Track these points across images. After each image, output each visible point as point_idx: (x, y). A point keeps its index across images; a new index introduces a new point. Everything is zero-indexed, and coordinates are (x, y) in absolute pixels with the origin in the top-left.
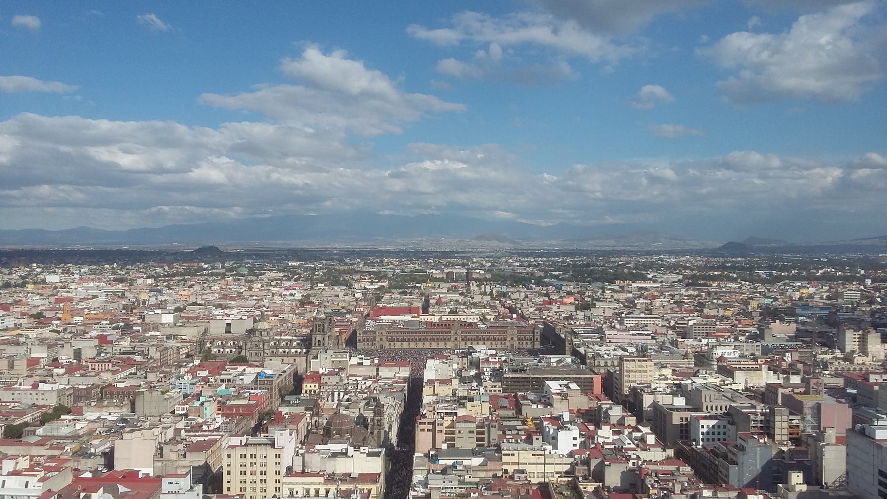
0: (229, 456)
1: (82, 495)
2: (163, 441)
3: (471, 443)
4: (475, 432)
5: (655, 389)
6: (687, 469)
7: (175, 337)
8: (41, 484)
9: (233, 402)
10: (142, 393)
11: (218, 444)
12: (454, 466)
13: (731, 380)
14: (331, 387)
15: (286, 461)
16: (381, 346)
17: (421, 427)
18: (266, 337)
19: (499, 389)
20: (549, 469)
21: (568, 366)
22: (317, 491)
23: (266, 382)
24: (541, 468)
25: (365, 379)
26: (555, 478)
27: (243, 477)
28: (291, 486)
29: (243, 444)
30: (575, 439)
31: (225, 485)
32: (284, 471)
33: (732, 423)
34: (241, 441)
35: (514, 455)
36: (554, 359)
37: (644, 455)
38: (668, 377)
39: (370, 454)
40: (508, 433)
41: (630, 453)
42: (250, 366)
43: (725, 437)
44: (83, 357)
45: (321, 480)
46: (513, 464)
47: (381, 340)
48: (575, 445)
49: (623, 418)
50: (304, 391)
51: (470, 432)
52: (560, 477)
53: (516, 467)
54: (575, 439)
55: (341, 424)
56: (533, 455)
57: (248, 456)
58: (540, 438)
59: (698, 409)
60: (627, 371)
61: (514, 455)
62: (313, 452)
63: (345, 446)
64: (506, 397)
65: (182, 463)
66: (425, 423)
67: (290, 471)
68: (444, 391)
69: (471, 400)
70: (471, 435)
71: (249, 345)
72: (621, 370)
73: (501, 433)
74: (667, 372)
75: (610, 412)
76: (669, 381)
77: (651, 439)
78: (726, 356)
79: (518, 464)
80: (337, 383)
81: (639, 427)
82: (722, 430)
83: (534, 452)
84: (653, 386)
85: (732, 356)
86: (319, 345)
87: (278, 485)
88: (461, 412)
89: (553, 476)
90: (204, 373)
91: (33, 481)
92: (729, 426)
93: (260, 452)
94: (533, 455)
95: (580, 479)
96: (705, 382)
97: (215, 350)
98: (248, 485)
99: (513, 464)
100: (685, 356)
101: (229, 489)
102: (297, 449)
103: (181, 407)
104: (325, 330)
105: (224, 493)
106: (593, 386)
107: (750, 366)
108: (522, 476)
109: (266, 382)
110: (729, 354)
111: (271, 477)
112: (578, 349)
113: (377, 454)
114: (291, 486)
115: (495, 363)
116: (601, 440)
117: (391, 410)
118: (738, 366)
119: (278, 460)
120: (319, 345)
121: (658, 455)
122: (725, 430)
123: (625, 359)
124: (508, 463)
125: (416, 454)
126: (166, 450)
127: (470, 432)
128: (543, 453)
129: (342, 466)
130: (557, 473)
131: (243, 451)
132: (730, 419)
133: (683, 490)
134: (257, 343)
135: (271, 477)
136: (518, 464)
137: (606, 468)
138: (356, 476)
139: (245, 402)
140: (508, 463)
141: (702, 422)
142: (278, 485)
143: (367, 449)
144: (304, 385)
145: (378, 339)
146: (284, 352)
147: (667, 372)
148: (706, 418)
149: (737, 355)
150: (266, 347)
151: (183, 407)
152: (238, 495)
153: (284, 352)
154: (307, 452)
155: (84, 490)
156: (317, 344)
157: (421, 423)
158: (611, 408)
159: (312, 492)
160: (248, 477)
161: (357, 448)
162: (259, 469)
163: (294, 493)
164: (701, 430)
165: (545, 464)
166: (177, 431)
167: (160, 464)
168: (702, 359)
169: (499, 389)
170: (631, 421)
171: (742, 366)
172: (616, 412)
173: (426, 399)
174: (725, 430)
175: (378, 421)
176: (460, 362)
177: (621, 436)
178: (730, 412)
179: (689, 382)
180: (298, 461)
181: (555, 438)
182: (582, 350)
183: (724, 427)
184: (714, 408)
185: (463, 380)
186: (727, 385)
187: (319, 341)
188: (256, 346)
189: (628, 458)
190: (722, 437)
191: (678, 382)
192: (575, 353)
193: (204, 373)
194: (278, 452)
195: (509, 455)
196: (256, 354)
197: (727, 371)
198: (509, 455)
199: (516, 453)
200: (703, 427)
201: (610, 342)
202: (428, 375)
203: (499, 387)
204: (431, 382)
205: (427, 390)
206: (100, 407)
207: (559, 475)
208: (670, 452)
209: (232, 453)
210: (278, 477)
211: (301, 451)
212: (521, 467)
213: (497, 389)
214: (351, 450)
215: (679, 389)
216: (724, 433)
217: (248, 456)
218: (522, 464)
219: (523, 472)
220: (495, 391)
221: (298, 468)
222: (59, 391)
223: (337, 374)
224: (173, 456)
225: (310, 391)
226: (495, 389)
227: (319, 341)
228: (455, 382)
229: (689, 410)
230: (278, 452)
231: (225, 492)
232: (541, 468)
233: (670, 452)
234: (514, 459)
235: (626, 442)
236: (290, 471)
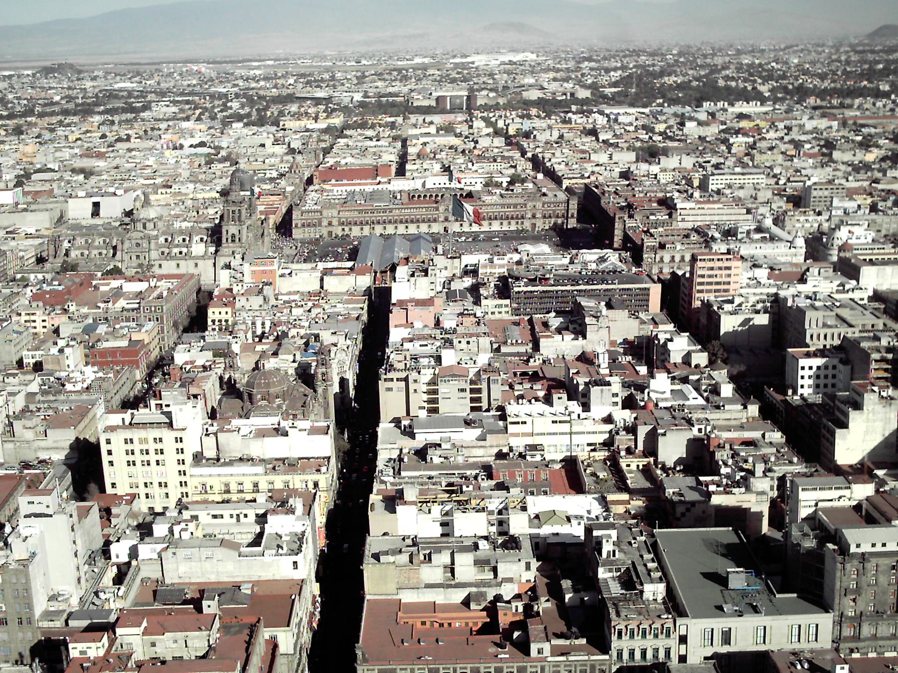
0: (108, 442)
2: (11, 413)
3: (461, 405)
4: (468, 390)
6: (777, 436)
9: (106, 345)
11: (90, 415)
13: (854, 282)
14: (250, 313)
15: (191, 446)
18: (152, 230)
19: (507, 309)
20: (576, 439)
23: (153, 309)
29: (127, 423)
30: (616, 395)
32: (189, 459)
33: (844, 362)
35: (525, 423)
39: (313, 431)
43: (834, 381)
49: (688, 355)
50: (210, 323)
51: (463, 390)
52: (592, 450)
54: (616, 395)
55: (268, 385)
56: (553, 422)
61: (525, 423)
62: (229, 431)
64: (517, 324)
65: (43, 444)
66: (392, 380)
67: (198, 458)
70: (462, 394)
71: (127, 244)
72: (692, 273)
73: (507, 388)
74: (762, 274)
75: (670, 345)
77: (727, 390)
80: (261, 306)
82: (830, 372)
83: (555, 418)
85: (863, 241)
86: (233, 241)
87: (183, 479)
92: (841, 367)
94: (553, 422)
95: (623, 453)
97: (78, 252)
101: (113, 485)
102: (205, 427)
103: (31, 353)
104: (243, 218)
105: (108, 492)
106: (648, 300)
107: (886, 257)
109: (153, 309)
110: (858, 238)
117: (341, 356)
118: (868, 258)
121: (735, 412)
122: (834, 372)
123: (699, 257)
124: (516, 435)
126: (17, 425)
127: (463, 390)
128: (568, 418)
130: (589, 445)
131: (128, 434)
132: (843, 356)
134: (140, 241)
137: (660, 438)
140: (516, 435)
141: (803, 362)
142: (183, 479)
143: (306, 424)
146: (181, 253)
148: (808, 355)
149: (870, 240)
150: (153, 246)
151: (34, 353)
152: (127, 495)
153: (181, 253)
154: (222, 430)
156: (230, 240)
157: (385, 380)
158: (671, 340)
163: (208, 488)
164: (801, 373)
165: (571, 433)
166: (30, 396)
167: (10, 446)
169: (507, 309)
171: (874, 258)
174: (834, 372)
175: (323, 374)
178: (845, 344)
180: (210, 442)
181: (586, 395)
183: (834, 367)
184: (822, 337)
187: (233, 236)
188: (138, 245)
195: (518, 423)
196: (138, 257)
198: (518, 423)
199: (529, 420)
200: (803, 368)
203: (506, 306)
204: (402, 304)
205: (396, 317)
207: (593, 447)
208: (754, 409)
209: (113, 436)
210: (182, 468)
211: (211, 429)
213: (504, 309)
215: (774, 305)
216: (834, 376)
218: (538, 434)
220: (500, 313)
221: (210, 453)
226: (500, 310)
227: (233, 236)
228: (439, 302)
230: (178, 434)
231: (109, 490)
235: (690, 397)
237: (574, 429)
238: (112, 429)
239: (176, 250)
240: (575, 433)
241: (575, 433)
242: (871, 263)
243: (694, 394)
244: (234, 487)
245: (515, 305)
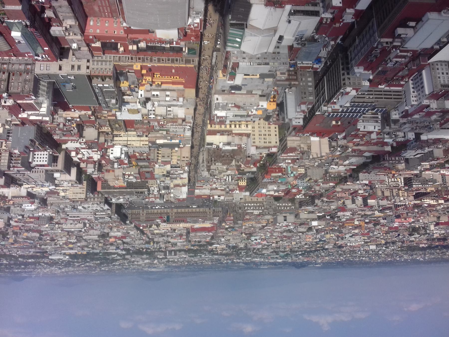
0: (276, 142)
1: (339, 123)
5: (69, 183)
6: (56, 137)
7: (310, 212)
8: (358, 128)
10: (321, 179)
12: (171, 139)
13: (28, 190)
15: (251, 140)
16: (210, 209)
17: (187, 159)
20: (125, 138)
21: (114, 196)
22: (235, 126)
24: (130, 139)
25: (216, 189)
26: (122, 133)
27: (269, 133)
28: (247, 129)
30: (112, 153)
31: (277, 129)
36: (121, 201)
37: (77, 145)
38: (62, 191)
39: (212, 144)
40: (145, 157)
41: (84, 146)
42: (272, 195)
44: (351, 200)
45: (233, 132)
46: (143, 141)
47: (210, 213)
48: (112, 150)
53: (142, 139)
57: (268, 142)
58: (129, 153)
59: (47, 171)
60: (83, 193)
62: (238, 145)
63: (223, 148)
64: (146, 178)
65: (298, 142)
68: (178, 181)
69: (164, 175)
72: (86, 194)
74: (62, 194)
75: (93, 170)
76: (61, 188)
77: (73, 154)
78: (30, 205)
79: (141, 141)
81: (78, 161)
84: (70, 185)
85: (26, 205)
86: (240, 207)
88: (168, 167)
89: (124, 135)
90: (294, 191)
91: (362, 129)
93: (262, 144)
95: (110, 133)
96: (42, 188)
98: (267, 129)
99: (143, 141)
100: (52, 204)
101: (275, 128)
108: (139, 134)
110: (28, 206)
111: (257, 133)
112: (109, 208)
113: (208, 144)
114: (247, 129)
115: (152, 198)
116: (99, 153)
118: (24, 199)
120: (240, 207)
121: (70, 145)
124: (146, 141)
125: (190, 145)
129: (225, 138)
130: (121, 137)
131: (270, 145)
133: (58, 125)
135: (257, 133)
136: (141, 141)
138: (218, 134)
140: (146, 141)
142: (253, 129)
143: (214, 146)
144: (246, 184)
145: (211, 213)
147: (62, 194)
149: (24, 205)
155: (339, 125)
158: (93, 172)
159: (237, 126)
160: (267, 133)
161: (218, 147)
162: (263, 137)
164: (47, 159)
165: (127, 141)
168: (44, 202)
170: (82, 165)
172: (90, 170)
173: (186, 175)
176: (169, 198)
177: (88, 156)
179: (51, 188)
182: (106, 207)
184: (39, 172)
185: (167, 188)
186: (31, 187)
187: (240, 209)
189: (85, 143)
191: (57, 188)
192: (110, 204)
193: (294, 191)
194: (254, 144)
197: (31, 196)
199: (141, 146)
200: (46, 161)
201: (91, 212)
202: (185, 189)
204: (184, 185)
205: (186, 181)
206: (339, 172)
208: (64, 146)
210: (254, 133)
212: (139, 138)
213: (151, 183)
214: (221, 146)
217: (268, 142)
219: (138, 136)
222: (358, 180)
223: (230, 190)
227: (240, 209)
228: (172, 186)
229: (52, 171)
230: (254, 144)
231: (277, 126)
232: (130, 139)
233: (64, 146)
234: (142, 143)
236: (248, 135)
237: (126, 142)
238: (275, 147)
239: (258, 205)
242: (23, 197)
243: (84, 153)
244: (237, 126)
245: (147, 184)
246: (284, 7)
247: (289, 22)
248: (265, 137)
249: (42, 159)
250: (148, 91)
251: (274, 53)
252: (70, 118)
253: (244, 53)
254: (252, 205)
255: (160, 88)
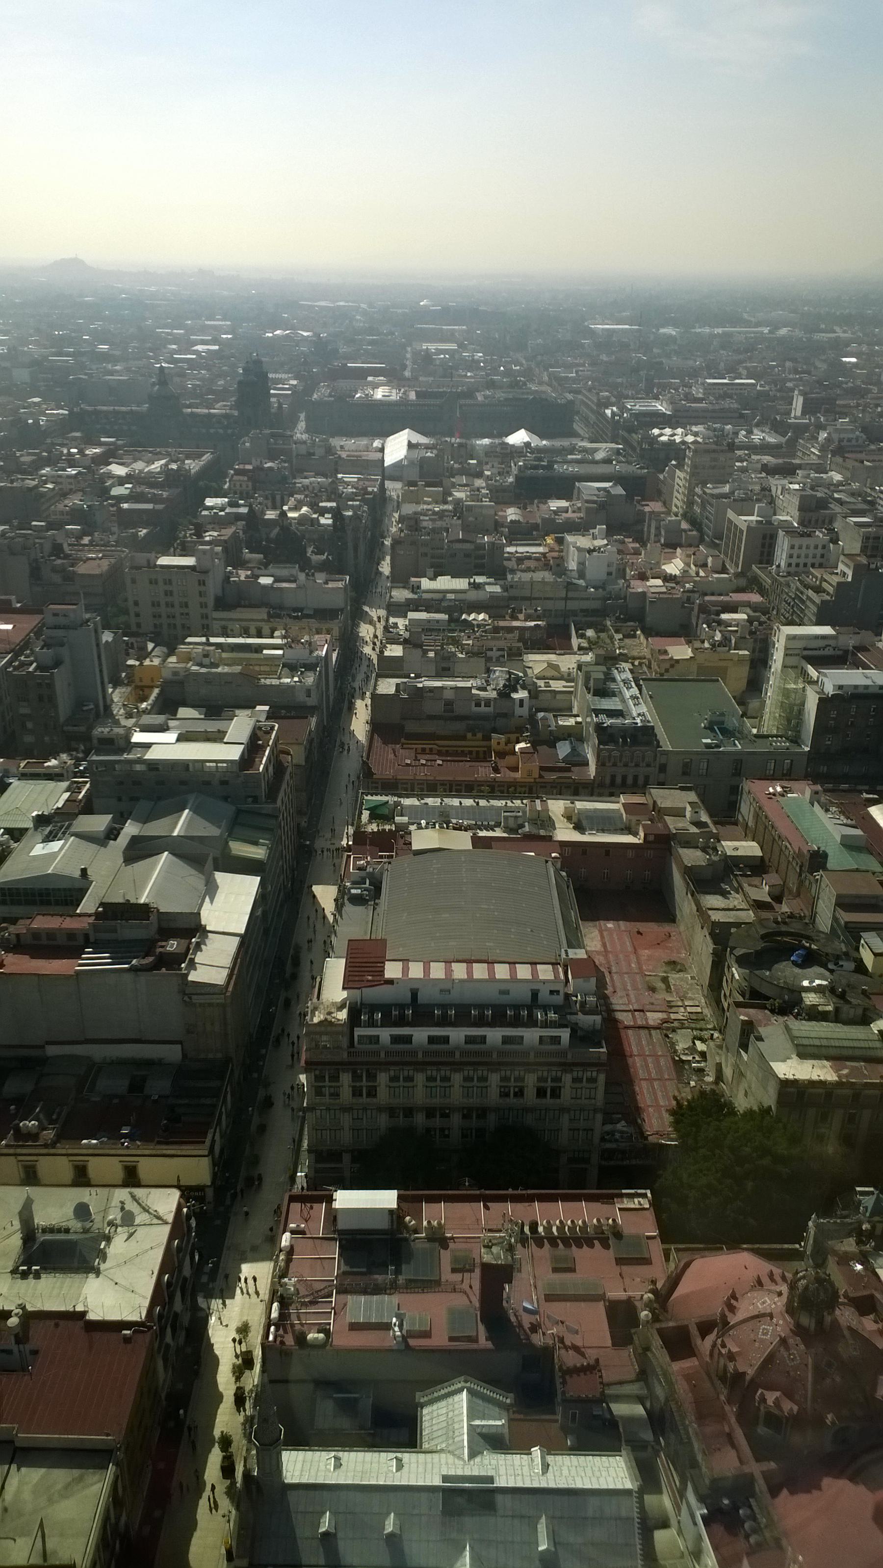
0: (134, 581)
28: (223, 623)
32: (211, 603)
34: (148, 561)
43: (821, 560)
51: (467, 555)
52: (585, 616)
85: (854, 442)
101: (139, 625)
110: (849, 440)
114: (223, 623)
119: (202, 588)
130: (582, 611)
139: (150, 506)
142: (205, 622)
152: (152, 633)
165: (566, 599)
190: (818, 560)
201: (677, 422)
210: (204, 611)
224: (57, 578)
225: (241, 493)
232: (560, 605)
237: (570, 594)
240: (572, 599)
241: (572, 599)
246: (102, 904)
247: (84, 872)
248: (170, 599)
249: (804, 551)
250: (505, 715)
251: (136, 799)
252: (719, 649)
253: (225, 799)
254: (212, 431)
255: (471, 722)
